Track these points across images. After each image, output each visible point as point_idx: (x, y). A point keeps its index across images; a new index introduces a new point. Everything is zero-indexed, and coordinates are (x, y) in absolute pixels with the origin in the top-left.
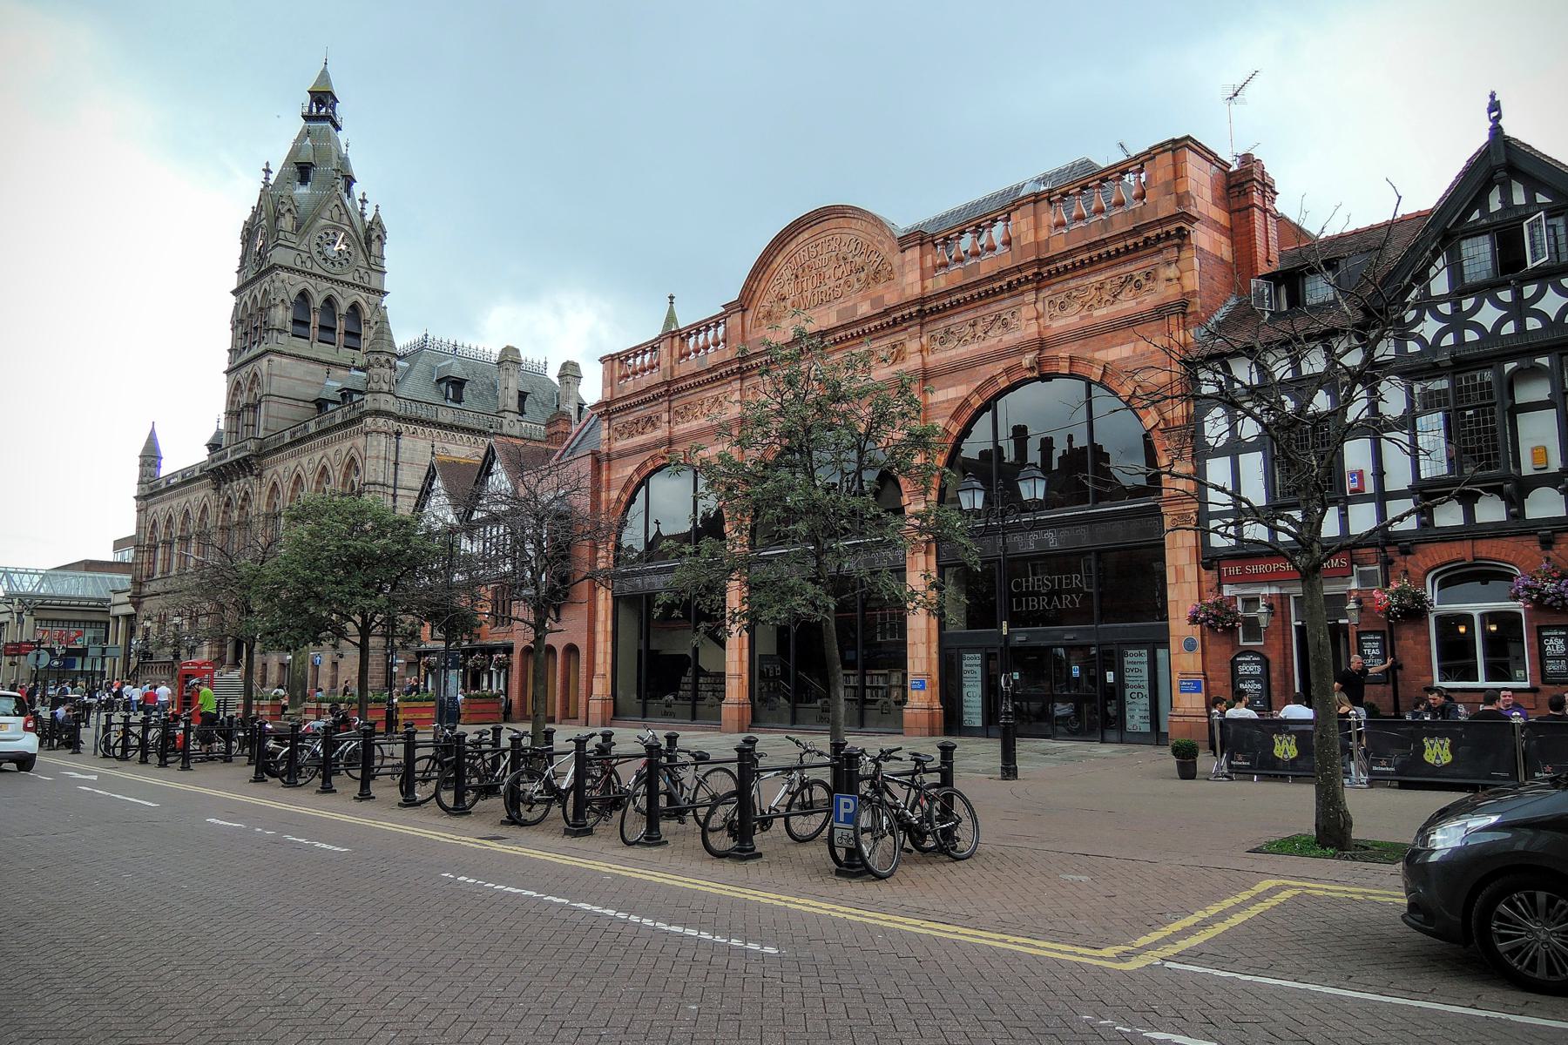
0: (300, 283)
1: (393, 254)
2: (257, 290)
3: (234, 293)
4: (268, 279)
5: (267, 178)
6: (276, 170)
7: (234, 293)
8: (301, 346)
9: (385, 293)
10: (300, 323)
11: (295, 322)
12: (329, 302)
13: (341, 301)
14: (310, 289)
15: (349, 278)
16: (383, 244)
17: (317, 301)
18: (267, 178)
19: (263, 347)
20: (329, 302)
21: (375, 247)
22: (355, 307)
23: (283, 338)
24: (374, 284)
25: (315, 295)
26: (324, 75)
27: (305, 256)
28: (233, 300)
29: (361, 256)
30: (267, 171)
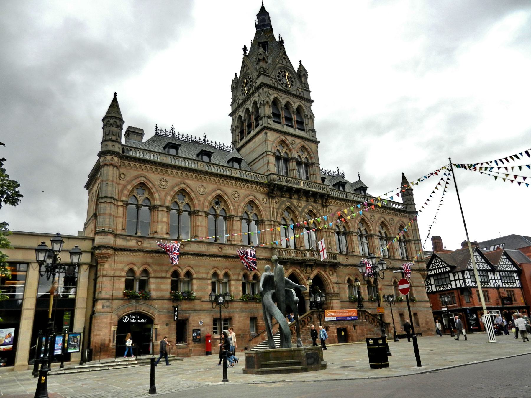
0: (273, 95)
1: (312, 82)
2: (249, 105)
3: (230, 115)
4: (257, 95)
5: (245, 53)
6: (249, 48)
7: (230, 115)
8: (277, 126)
9: (312, 101)
10: (276, 115)
11: (273, 113)
12: (288, 106)
13: (293, 103)
14: (278, 97)
15: (295, 93)
16: (307, 78)
17: (283, 103)
18: (245, 53)
19: (259, 128)
20: (288, 106)
21: (303, 79)
22: (299, 108)
23: (270, 121)
24: (305, 97)
25: (281, 100)
26: (263, 9)
27: (274, 80)
28: (230, 119)
29: (298, 83)
30: (245, 49)
